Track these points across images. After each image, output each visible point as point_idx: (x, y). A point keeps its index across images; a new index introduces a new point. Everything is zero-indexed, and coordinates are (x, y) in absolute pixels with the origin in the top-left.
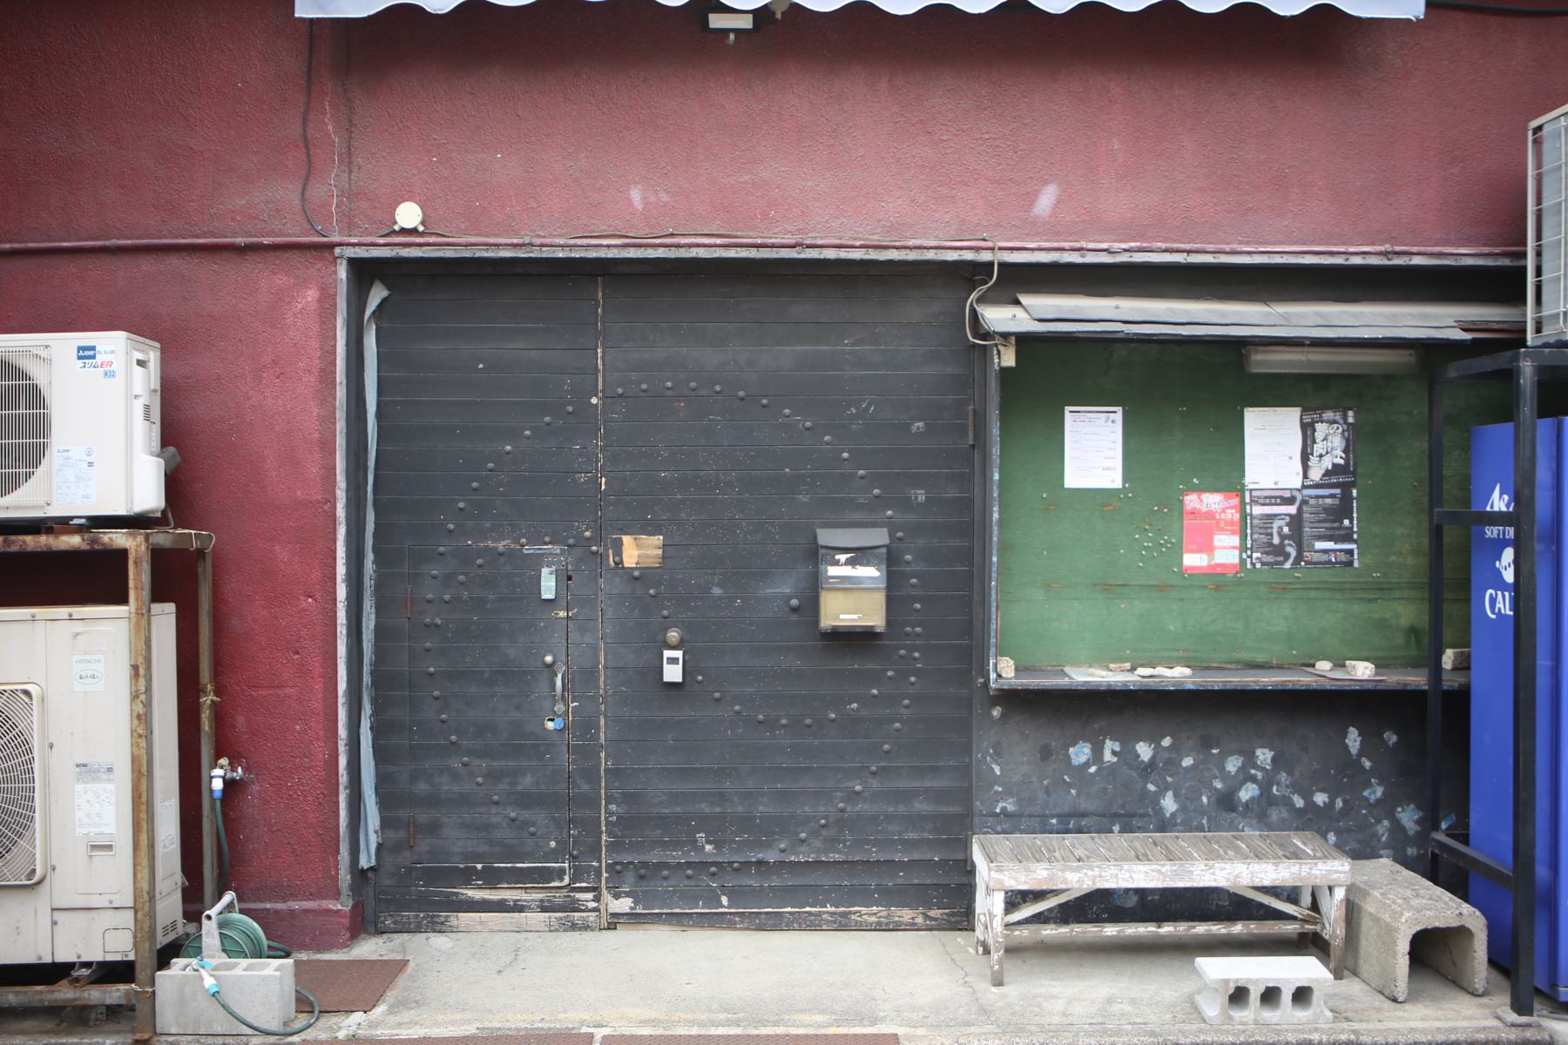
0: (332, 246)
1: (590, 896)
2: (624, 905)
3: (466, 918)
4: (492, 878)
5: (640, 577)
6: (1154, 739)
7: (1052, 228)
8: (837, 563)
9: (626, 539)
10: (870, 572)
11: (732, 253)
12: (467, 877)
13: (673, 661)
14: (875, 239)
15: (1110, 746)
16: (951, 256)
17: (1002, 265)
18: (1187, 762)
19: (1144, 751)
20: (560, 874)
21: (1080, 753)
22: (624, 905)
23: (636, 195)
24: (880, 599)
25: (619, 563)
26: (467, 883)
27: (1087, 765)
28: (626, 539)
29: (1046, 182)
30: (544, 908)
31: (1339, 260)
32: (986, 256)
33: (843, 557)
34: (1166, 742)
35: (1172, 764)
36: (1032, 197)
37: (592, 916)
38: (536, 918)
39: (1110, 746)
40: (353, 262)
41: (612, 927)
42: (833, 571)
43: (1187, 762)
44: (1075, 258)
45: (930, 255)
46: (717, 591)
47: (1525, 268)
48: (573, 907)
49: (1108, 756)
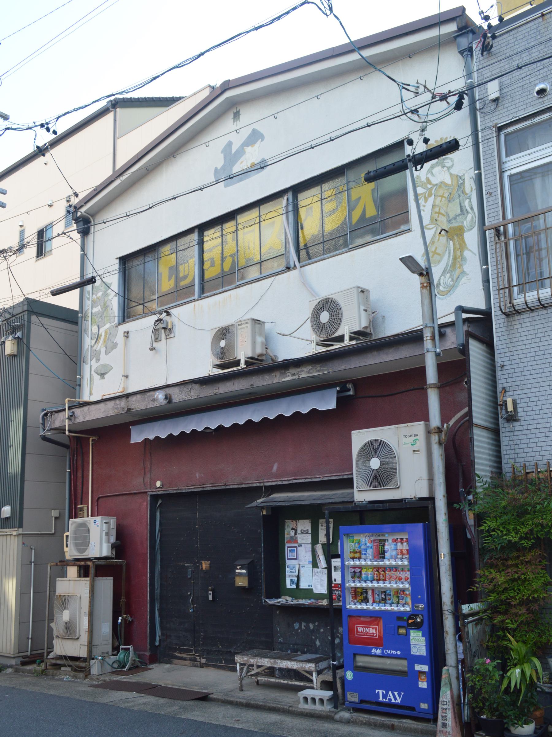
0: (146, 492)
1: (198, 658)
2: (203, 661)
3: (176, 661)
4: (181, 651)
5: (206, 572)
6: (314, 623)
7: (278, 475)
8: (237, 569)
9: (203, 562)
10: (244, 571)
11: (213, 488)
12: (175, 650)
13: (210, 594)
14: (239, 482)
16: (255, 485)
17: (265, 487)
18: (322, 630)
19: (311, 626)
20: (191, 651)
21: (296, 626)
22: (203, 661)
23: (197, 475)
24: (247, 578)
25: (202, 568)
26: (175, 651)
27: (298, 629)
28: (203, 562)
29: (275, 462)
30: (191, 660)
31: (341, 477)
32: (262, 484)
33: (239, 567)
34: (317, 624)
35: (318, 630)
36: (272, 467)
37: (199, 663)
38: (188, 663)
39: (303, 624)
40: (151, 496)
41: (202, 667)
42: (237, 571)
43: (322, 630)
44: (280, 483)
45: (251, 485)
46: (220, 576)
47: (352, 478)
48: (195, 660)
49: (303, 627)
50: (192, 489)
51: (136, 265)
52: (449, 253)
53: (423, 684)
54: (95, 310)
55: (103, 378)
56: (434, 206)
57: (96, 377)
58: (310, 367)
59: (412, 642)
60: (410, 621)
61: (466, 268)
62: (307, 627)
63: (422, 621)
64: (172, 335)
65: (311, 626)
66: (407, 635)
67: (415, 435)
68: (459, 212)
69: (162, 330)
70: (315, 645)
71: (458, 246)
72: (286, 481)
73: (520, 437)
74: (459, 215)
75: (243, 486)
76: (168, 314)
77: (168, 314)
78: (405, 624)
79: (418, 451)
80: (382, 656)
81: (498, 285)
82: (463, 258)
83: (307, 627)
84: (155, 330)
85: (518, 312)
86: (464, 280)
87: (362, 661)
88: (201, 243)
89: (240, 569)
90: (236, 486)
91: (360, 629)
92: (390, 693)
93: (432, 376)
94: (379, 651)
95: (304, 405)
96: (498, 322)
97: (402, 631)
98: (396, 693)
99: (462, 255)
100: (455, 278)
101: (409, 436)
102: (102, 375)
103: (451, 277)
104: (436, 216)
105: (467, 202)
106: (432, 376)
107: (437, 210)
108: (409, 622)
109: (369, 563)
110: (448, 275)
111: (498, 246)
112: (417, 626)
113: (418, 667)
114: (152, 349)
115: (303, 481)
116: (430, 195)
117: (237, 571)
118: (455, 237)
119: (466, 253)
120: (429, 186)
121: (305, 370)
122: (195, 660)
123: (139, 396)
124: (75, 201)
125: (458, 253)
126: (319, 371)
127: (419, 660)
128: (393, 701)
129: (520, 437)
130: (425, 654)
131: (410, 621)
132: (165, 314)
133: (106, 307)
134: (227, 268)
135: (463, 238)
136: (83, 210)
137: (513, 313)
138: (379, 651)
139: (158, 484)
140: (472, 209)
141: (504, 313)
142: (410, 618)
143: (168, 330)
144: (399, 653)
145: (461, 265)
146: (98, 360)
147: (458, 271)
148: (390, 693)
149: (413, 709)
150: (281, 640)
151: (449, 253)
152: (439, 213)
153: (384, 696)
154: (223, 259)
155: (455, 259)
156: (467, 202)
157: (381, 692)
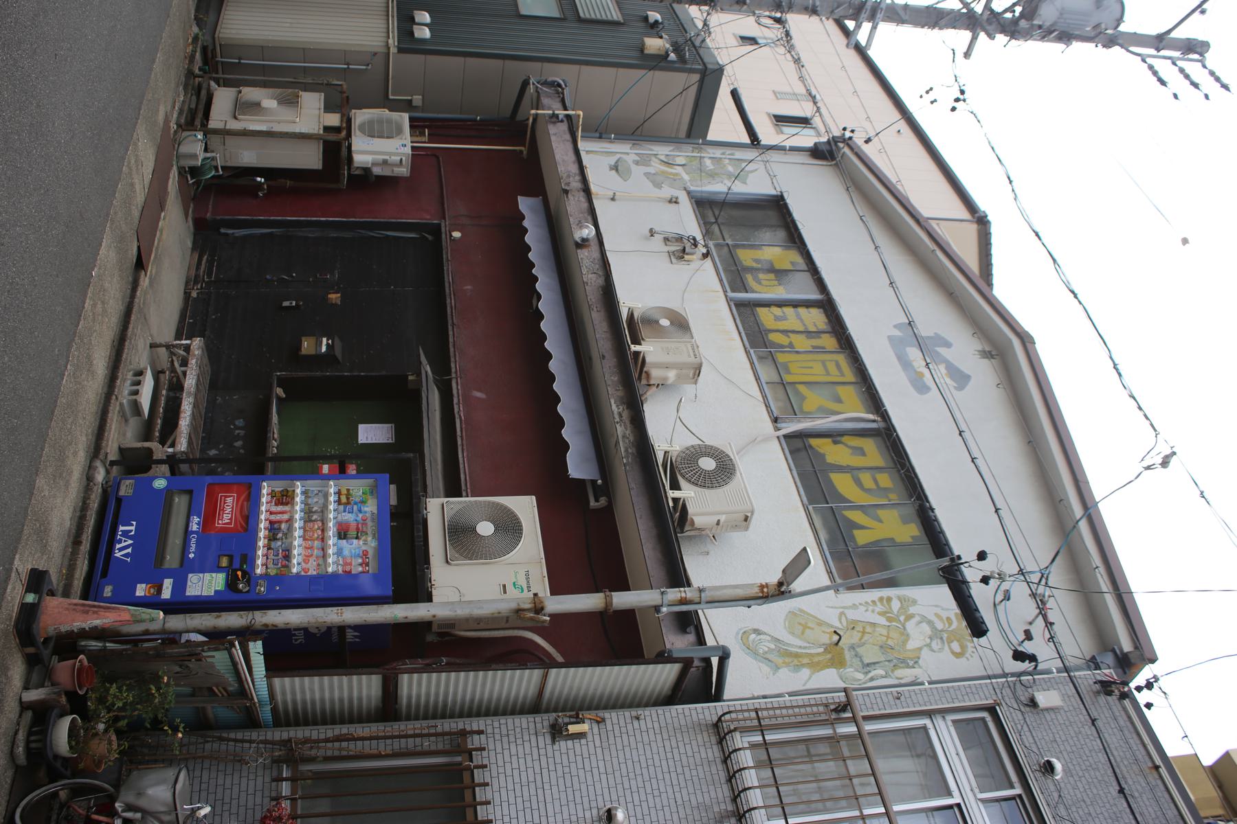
2: (194, 294)
3: (196, 256)
4: (210, 263)
5: (325, 299)
6: (243, 447)
10: (324, 349)
15: (242, 432)
16: (453, 365)
17: (450, 380)
20: (209, 275)
21: (240, 422)
22: (194, 294)
30: (196, 276)
36: (479, 390)
38: (193, 273)
39: (242, 432)
40: (439, 225)
42: (324, 340)
44: (455, 401)
47: (461, 496)
50: (448, 278)
51: (772, 215)
52: (805, 648)
53: (141, 590)
54: (708, 162)
55: (611, 169)
56: (873, 625)
57: (612, 160)
58: (632, 438)
59: (207, 576)
60: (239, 573)
61: (784, 672)
62: (238, 438)
63: (241, 591)
64: (674, 260)
65: (238, 444)
66: (219, 569)
67: (529, 587)
68: (866, 661)
69: (681, 249)
70: (210, 449)
71: (816, 659)
72: (459, 410)
73: (527, 745)
74: (861, 661)
75: (452, 350)
76: (705, 256)
77: (705, 256)
78: (236, 565)
79: (505, 592)
80: (187, 532)
81: (762, 709)
82: (798, 668)
83: (238, 438)
84: (680, 239)
85: (721, 741)
86: (766, 669)
87: (180, 502)
88: (808, 304)
89: (328, 344)
90: (451, 340)
91: (229, 500)
92: (130, 542)
93: (622, 600)
94: (195, 527)
95: (573, 433)
96: (706, 711)
97: (224, 562)
98: (129, 550)
99: (803, 665)
100: (768, 656)
101: (528, 579)
102: (615, 168)
103: (771, 651)
104: (859, 628)
105: (881, 672)
106: (622, 600)
107: (868, 629)
108: (239, 571)
109: (331, 516)
110: (773, 646)
111: (821, 709)
112: (231, 584)
113: (168, 584)
114: (652, 233)
115: (459, 433)
116: (889, 619)
117: (324, 340)
118: (829, 656)
119: (805, 672)
120: (902, 618)
121: (628, 432)
122: (196, 282)
123: (585, 205)
124: (859, 140)
125: (806, 661)
126: (626, 450)
127: (180, 586)
128: (118, 546)
129: (527, 745)
130: (188, 594)
131: (239, 573)
132: (704, 251)
133: (712, 175)
134: (773, 337)
135: (828, 667)
136: (846, 150)
137: (720, 732)
138: (195, 527)
139: (457, 234)
140: (872, 679)
141: (720, 719)
142: (244, 573)
143: (681, 255)
144: (192, 556)
145: (788, 665)
146: (637, 163)
147: (779, 661)
148: (130, 542)
149: (104, 574)
150: (219, 399)
151: (805, 648)
152: (864, 633)
153: (125, 534)
154: (785, 332)
155: (797, 655)
156: (881, 672)
157: (133, 528)
